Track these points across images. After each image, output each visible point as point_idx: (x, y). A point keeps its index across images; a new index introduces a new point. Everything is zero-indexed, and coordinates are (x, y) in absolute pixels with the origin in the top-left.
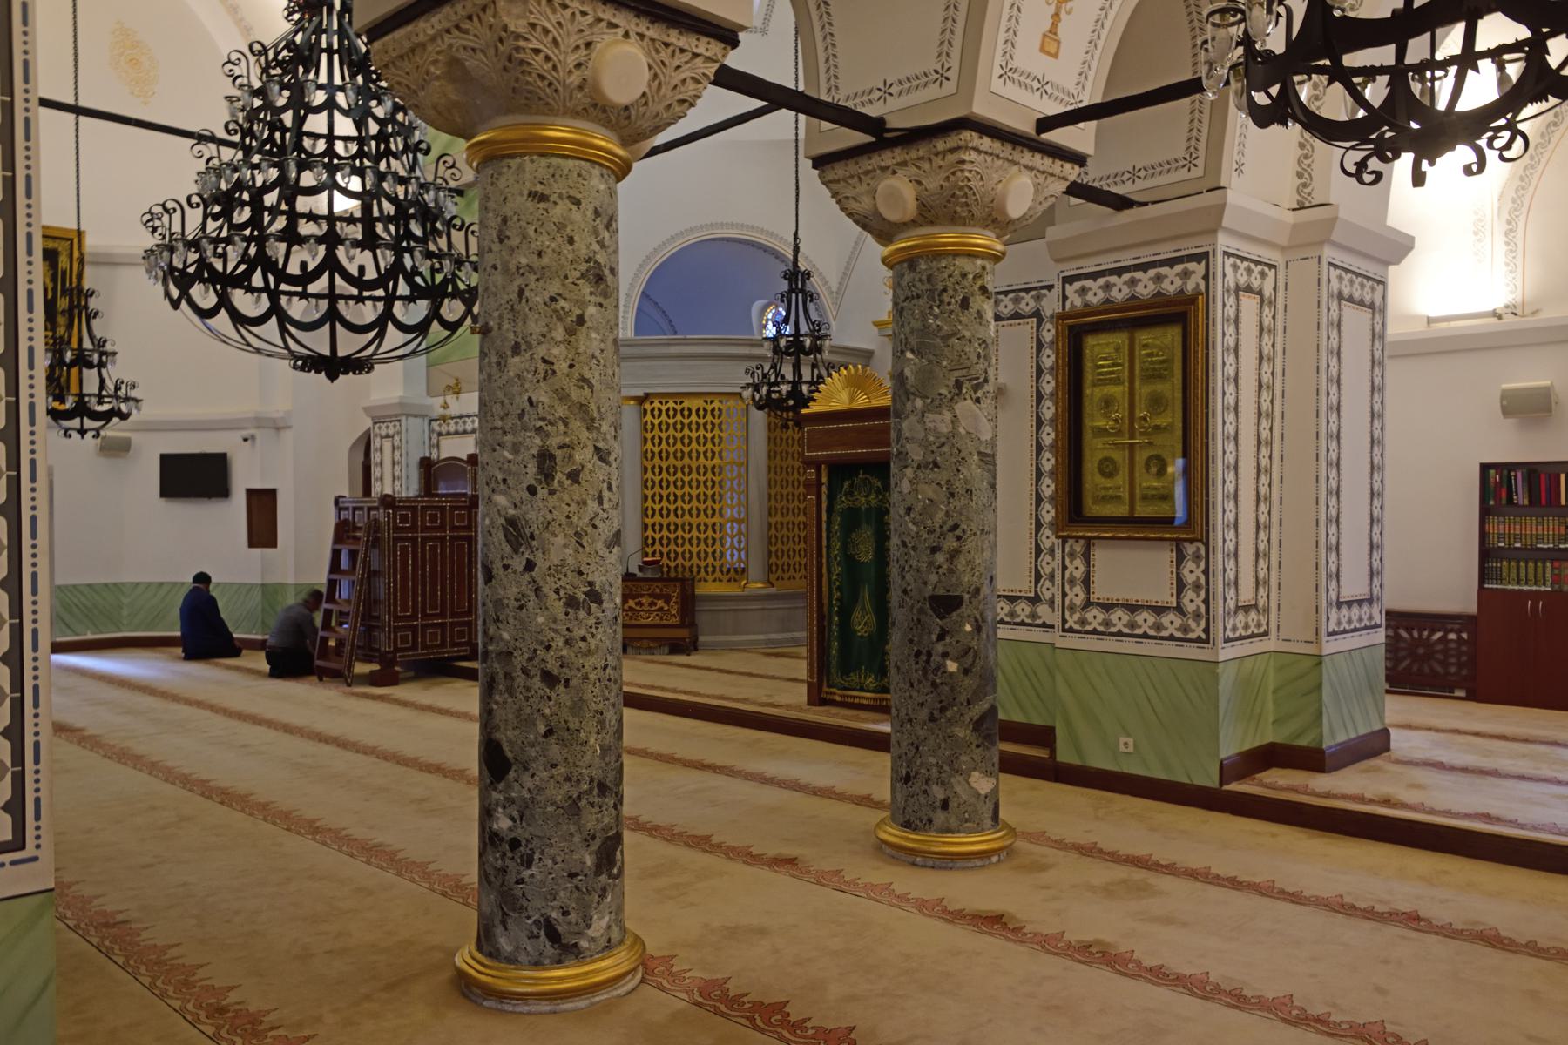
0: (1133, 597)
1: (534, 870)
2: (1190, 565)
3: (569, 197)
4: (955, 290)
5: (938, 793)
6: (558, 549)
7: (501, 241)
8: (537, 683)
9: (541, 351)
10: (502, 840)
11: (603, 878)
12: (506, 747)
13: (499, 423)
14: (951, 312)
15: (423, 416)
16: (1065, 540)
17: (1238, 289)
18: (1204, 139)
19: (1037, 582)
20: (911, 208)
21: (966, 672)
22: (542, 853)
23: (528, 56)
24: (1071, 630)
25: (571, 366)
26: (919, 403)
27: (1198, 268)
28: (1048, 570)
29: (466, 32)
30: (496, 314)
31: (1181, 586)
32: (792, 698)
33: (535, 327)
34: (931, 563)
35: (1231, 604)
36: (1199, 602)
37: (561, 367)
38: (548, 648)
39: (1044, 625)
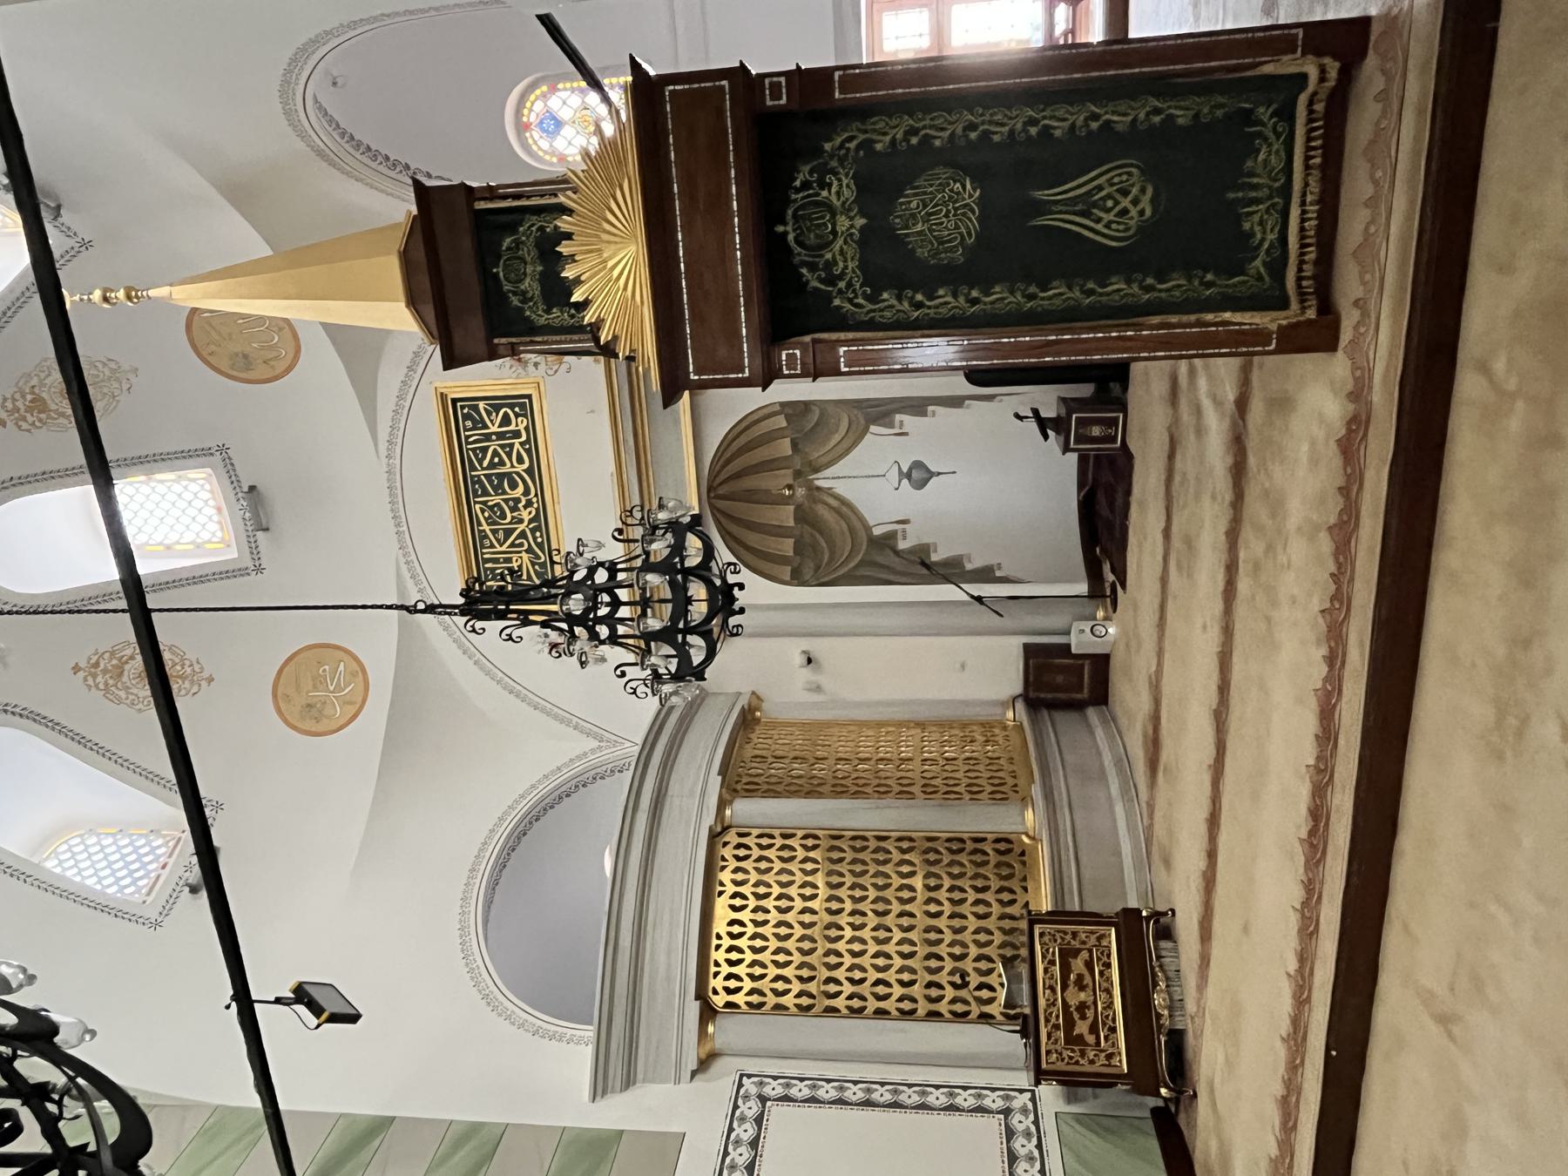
32: (1320, 407)
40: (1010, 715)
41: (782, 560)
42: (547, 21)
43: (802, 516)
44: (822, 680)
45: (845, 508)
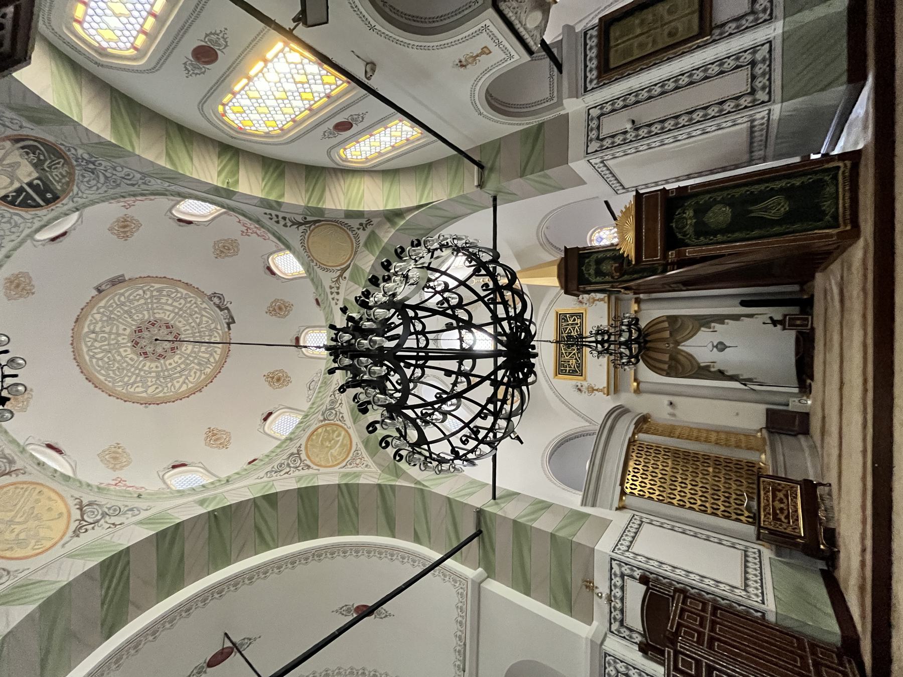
15: (606, 634)
19: (742, 66)
40: (759, 434)
41: (663, 370)
42: (606, 203)
43: (672, 358)
44: (676, 412)
45: (690, 357)
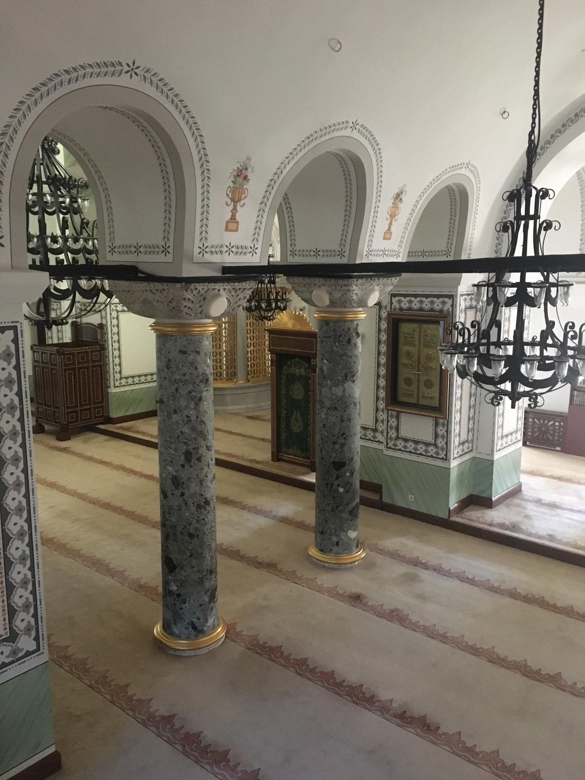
0: (417, 437)
1: (186, 605)
2: (441, 428)
3: (195, 351)
4: (345, 335)
5: (335, 539)
6: (194, 487)
7: (168, 369)
8: (186, 538)
9: (186, 412)
10: (173, 594)
11: (212, 604)
12: (174, 560)
13: (169, 439)
14: (343, 345)
16: (388, 410)
17: (466, 308)
18: (454, 243)
20: (327, 302)
21: (347, 492)
22: (190, 598)
23: (183, 308)
24: (390, 448)
25: (197, 417)
26: (329, 382)
27: (450, 302)
28: (381, 418)
29: (155, 294)
30: (166, 397)
31: (436, 436)
33: (183, 403)
34: (333, 448)
35: (457, 443)
36: (443, 443)
37: (194, 418)
38: (190, 524)
39: (379, 442)
